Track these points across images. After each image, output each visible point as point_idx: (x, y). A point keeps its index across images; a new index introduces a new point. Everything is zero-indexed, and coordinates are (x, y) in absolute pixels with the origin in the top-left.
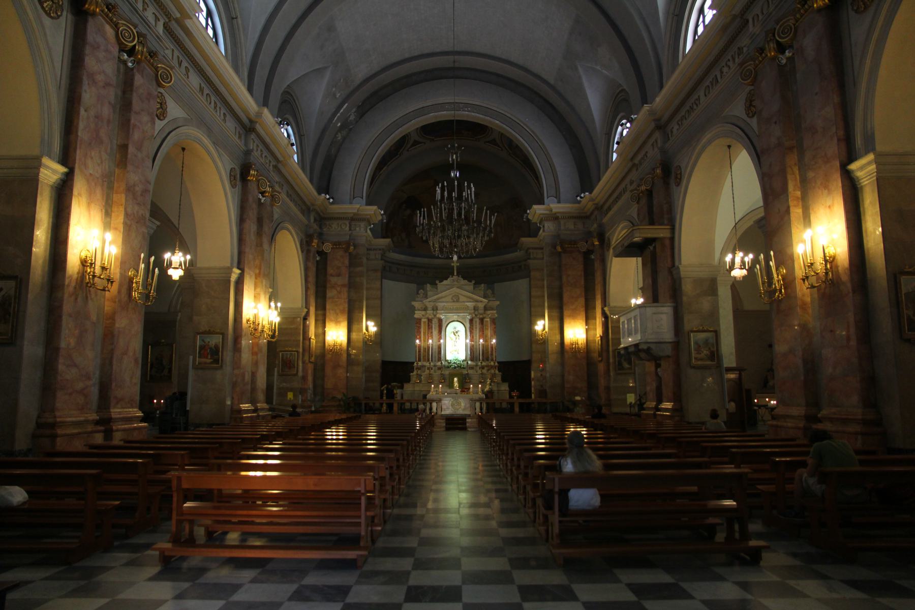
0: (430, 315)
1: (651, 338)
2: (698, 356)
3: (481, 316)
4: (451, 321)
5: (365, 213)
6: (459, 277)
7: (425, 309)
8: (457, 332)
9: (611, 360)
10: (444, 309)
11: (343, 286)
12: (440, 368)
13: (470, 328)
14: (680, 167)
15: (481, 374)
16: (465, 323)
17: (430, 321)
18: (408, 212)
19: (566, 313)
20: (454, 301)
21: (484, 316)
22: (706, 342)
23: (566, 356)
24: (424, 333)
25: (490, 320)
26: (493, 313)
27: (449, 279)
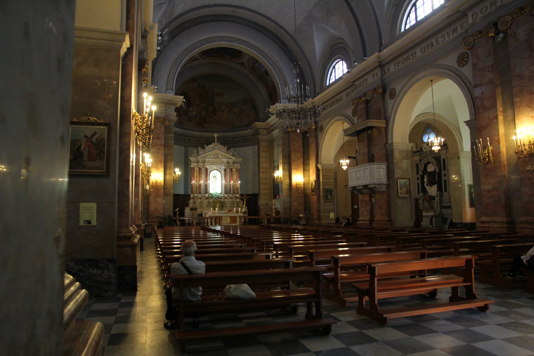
0: (201, 166)
1: (376, 181)
2: (401, 192)
3: (231, 167)
5: (175, 100)
7: (198, 162)
8: (215, 177)
9: (322, 194)
10: (209, 162)
11: (161, 145)
12: (207, 198)
13: (225, 174)
14: (394, 89)
15: (232, 202)
16: (221, 171)
17: (200, 169)
19: (293, 167)
20: (215, 158)
22: (405, 184)
23: (293, 191)
24: (197, 177)
25: (236, 170)
26: (238, 166)
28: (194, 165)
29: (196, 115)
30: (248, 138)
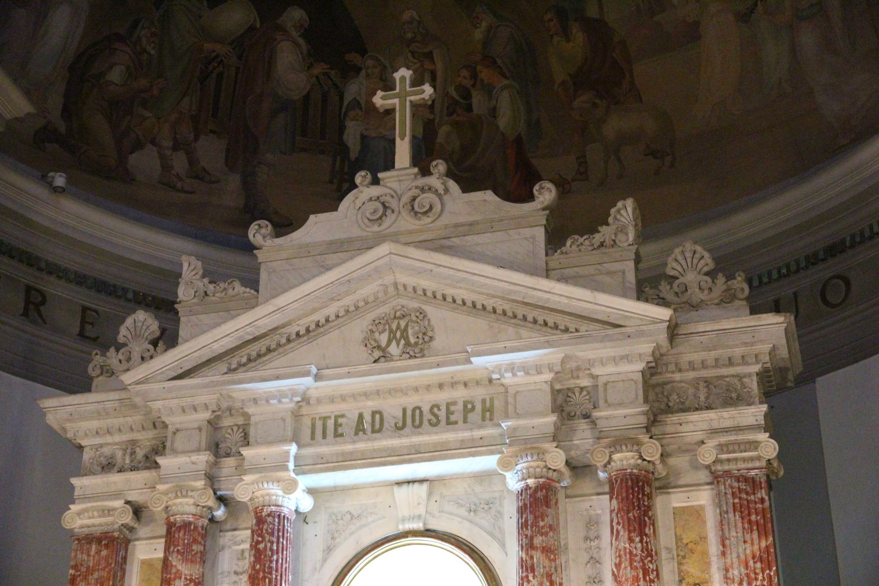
0: (181, 491)
3: (624, 459)
4: (368, 539)
6: (425, 172)
21: (652, 450)
27: (346, 203)
28: (116, 496)
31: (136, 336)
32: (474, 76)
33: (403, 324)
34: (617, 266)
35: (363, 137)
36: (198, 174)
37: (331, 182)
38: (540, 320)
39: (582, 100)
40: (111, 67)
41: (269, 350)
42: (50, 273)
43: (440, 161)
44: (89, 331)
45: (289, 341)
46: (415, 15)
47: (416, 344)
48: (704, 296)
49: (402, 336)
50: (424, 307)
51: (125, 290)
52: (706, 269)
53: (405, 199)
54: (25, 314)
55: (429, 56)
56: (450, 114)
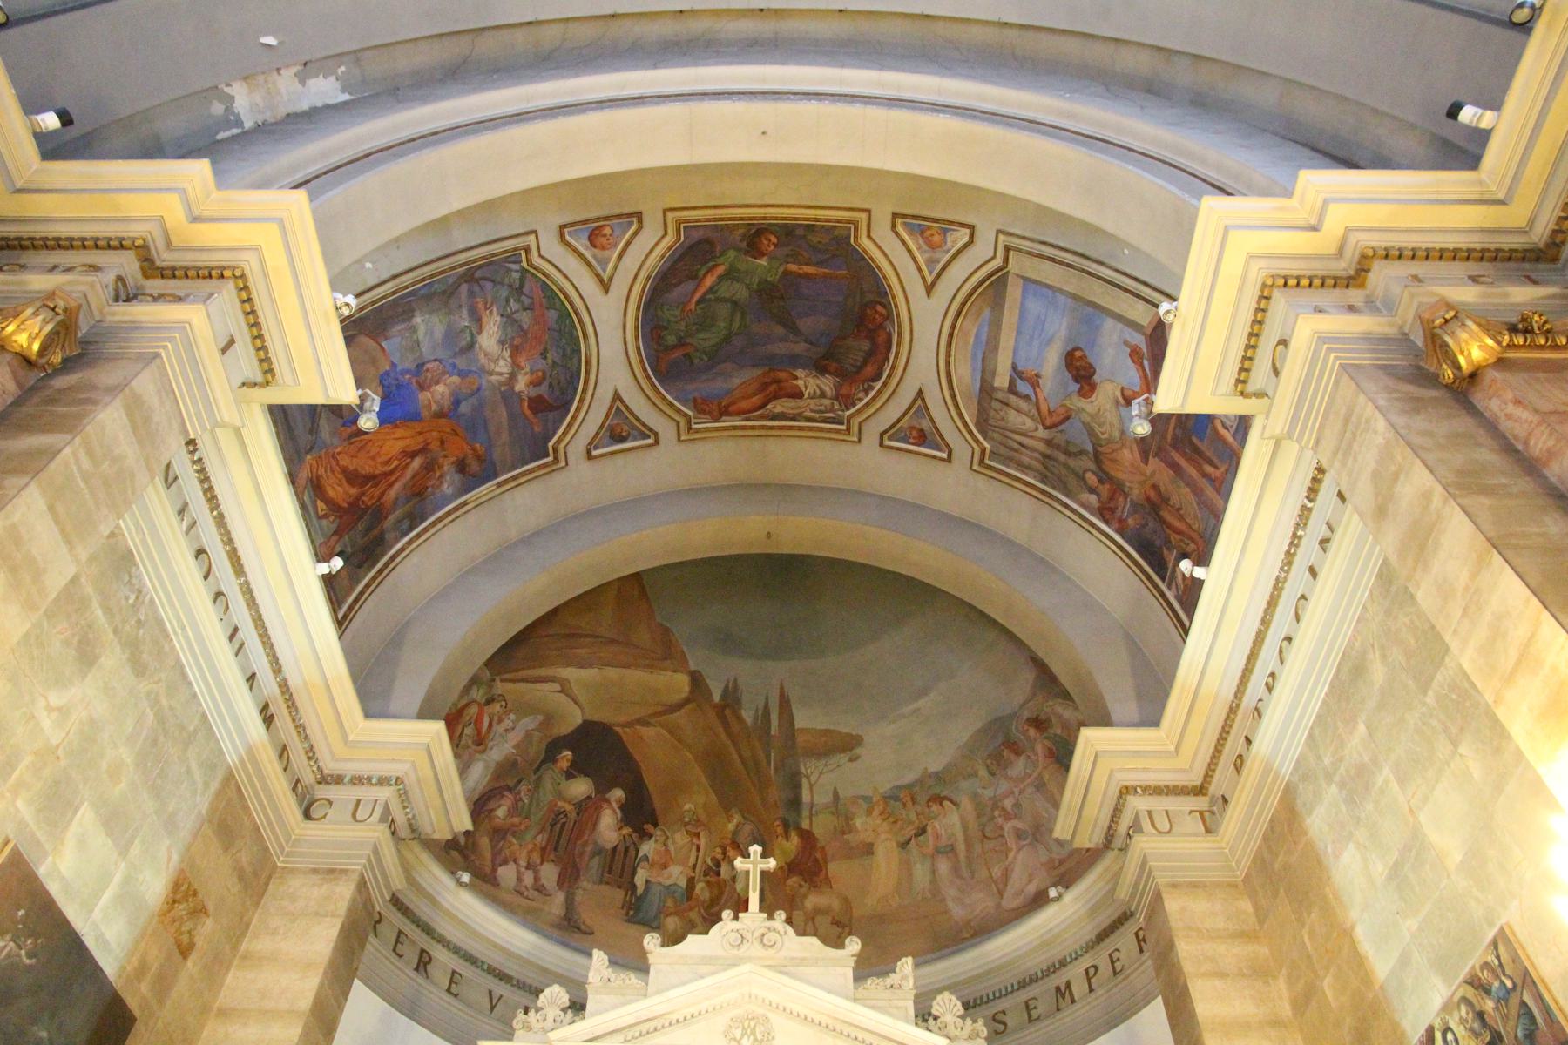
6: (771, 917)
18: (581, 787)
29: (691, 882)
30: (1068, 985)
31: (552, 1002)
32: (724, 853)
33: (752, 1024)
34: (901, 1003)
35: (647, 881)
36: (540, 889)
37: (622, 908)
38: (860, 1038)
39: (794, 880)
40: (499, 806)
41: (656, 1030)
42: (439, 942)
43: (782, 912)
44: (454, 989)
45: (670, 1024)
46: (693, 808)
47: (762, 1040)
48: (958, 1032)
49: (751, 1033)
50: (770, 1015)
51: (483, 962)
52: (959, 1013)
53: (757, 934)
54: (417, 969)
55: (697, 835)
56: (705, 875)
